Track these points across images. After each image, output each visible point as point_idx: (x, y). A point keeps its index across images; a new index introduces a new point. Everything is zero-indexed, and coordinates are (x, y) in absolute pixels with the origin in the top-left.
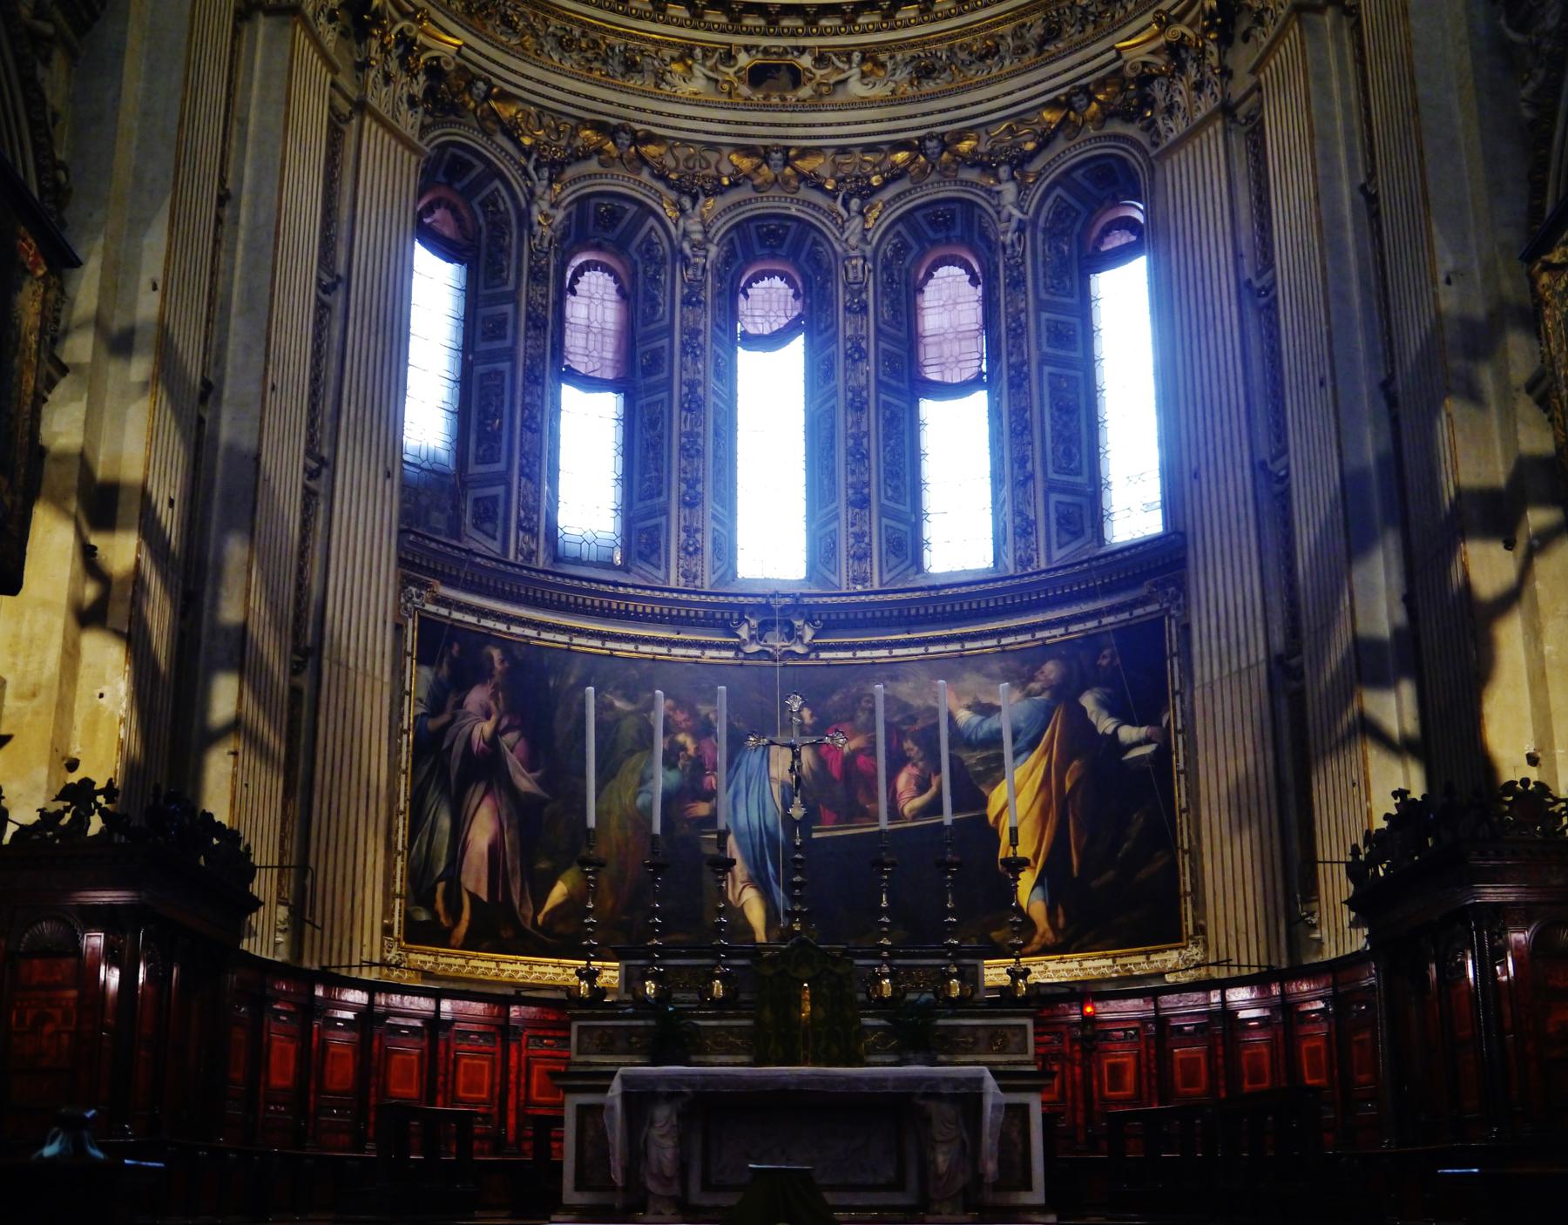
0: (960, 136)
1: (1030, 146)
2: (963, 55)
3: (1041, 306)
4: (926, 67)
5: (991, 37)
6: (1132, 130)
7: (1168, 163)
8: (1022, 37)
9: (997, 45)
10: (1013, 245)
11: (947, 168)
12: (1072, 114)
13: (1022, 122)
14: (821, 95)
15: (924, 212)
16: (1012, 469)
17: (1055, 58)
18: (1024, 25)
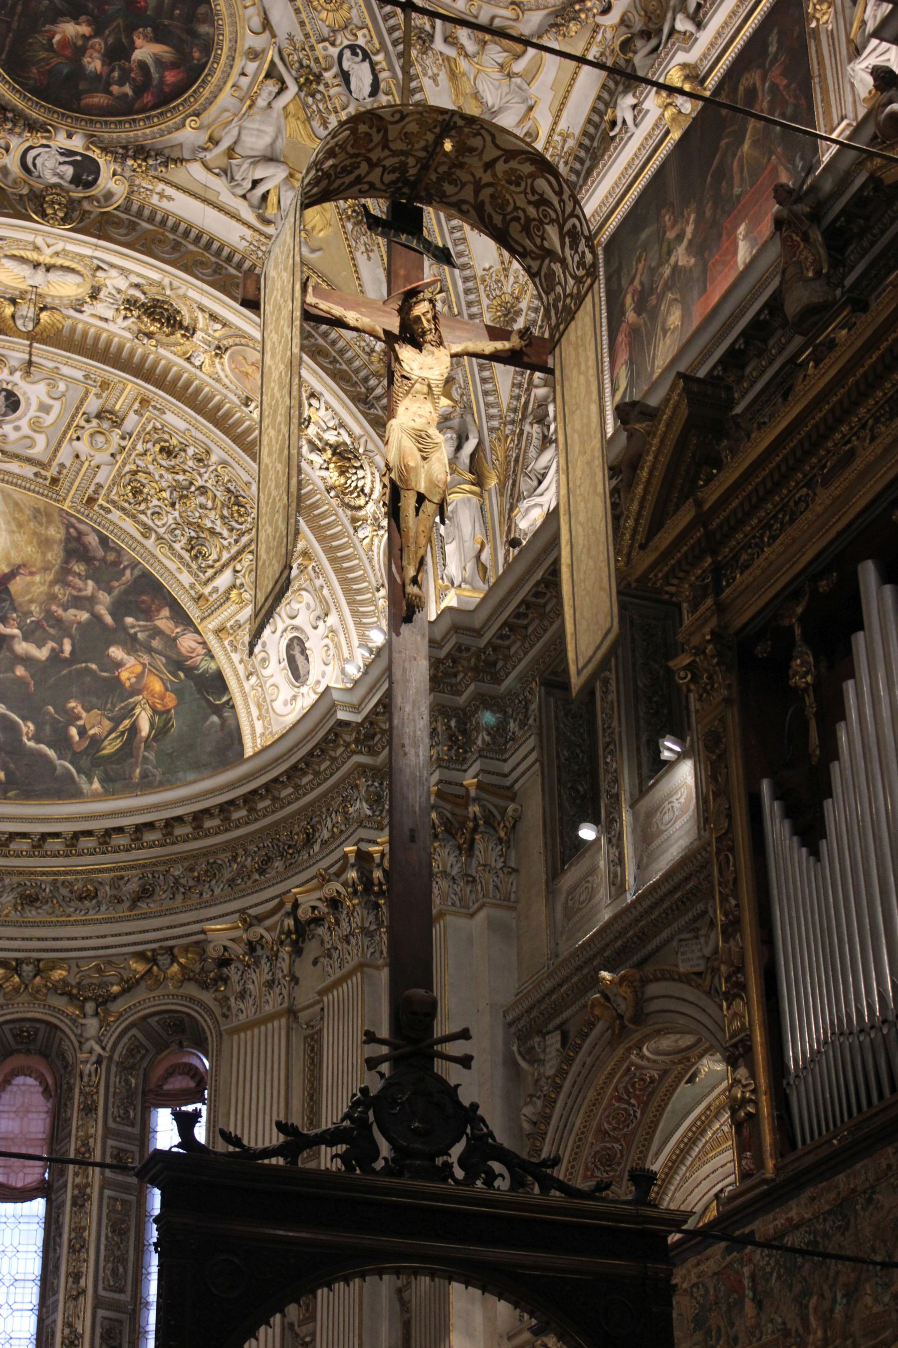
0: (54, 965)
1: (115, 989)
2: (64, 892)
3: (108, 1133)
4: (30, 896)
5: (91, 881)
6: (207, 997)
7: (235, 1037)
8: (118, 888)
9: (96, 890)
10: (90, 1075)
11: (38, 991)
12: (155, 968)
13: (110, 963)
14: (83, 1145)
15: (11, 1026)
16: (67, 1282)
17: (144, 917)
18: (122, 878)
